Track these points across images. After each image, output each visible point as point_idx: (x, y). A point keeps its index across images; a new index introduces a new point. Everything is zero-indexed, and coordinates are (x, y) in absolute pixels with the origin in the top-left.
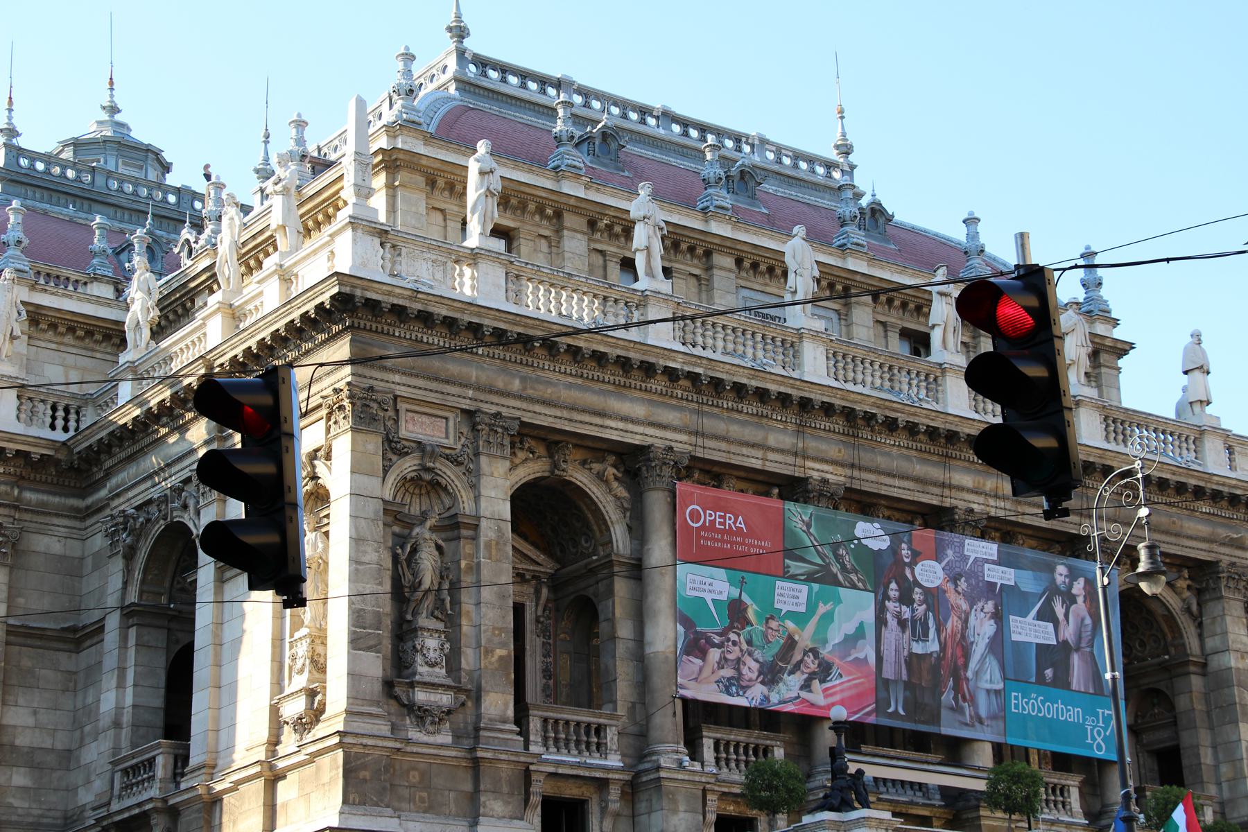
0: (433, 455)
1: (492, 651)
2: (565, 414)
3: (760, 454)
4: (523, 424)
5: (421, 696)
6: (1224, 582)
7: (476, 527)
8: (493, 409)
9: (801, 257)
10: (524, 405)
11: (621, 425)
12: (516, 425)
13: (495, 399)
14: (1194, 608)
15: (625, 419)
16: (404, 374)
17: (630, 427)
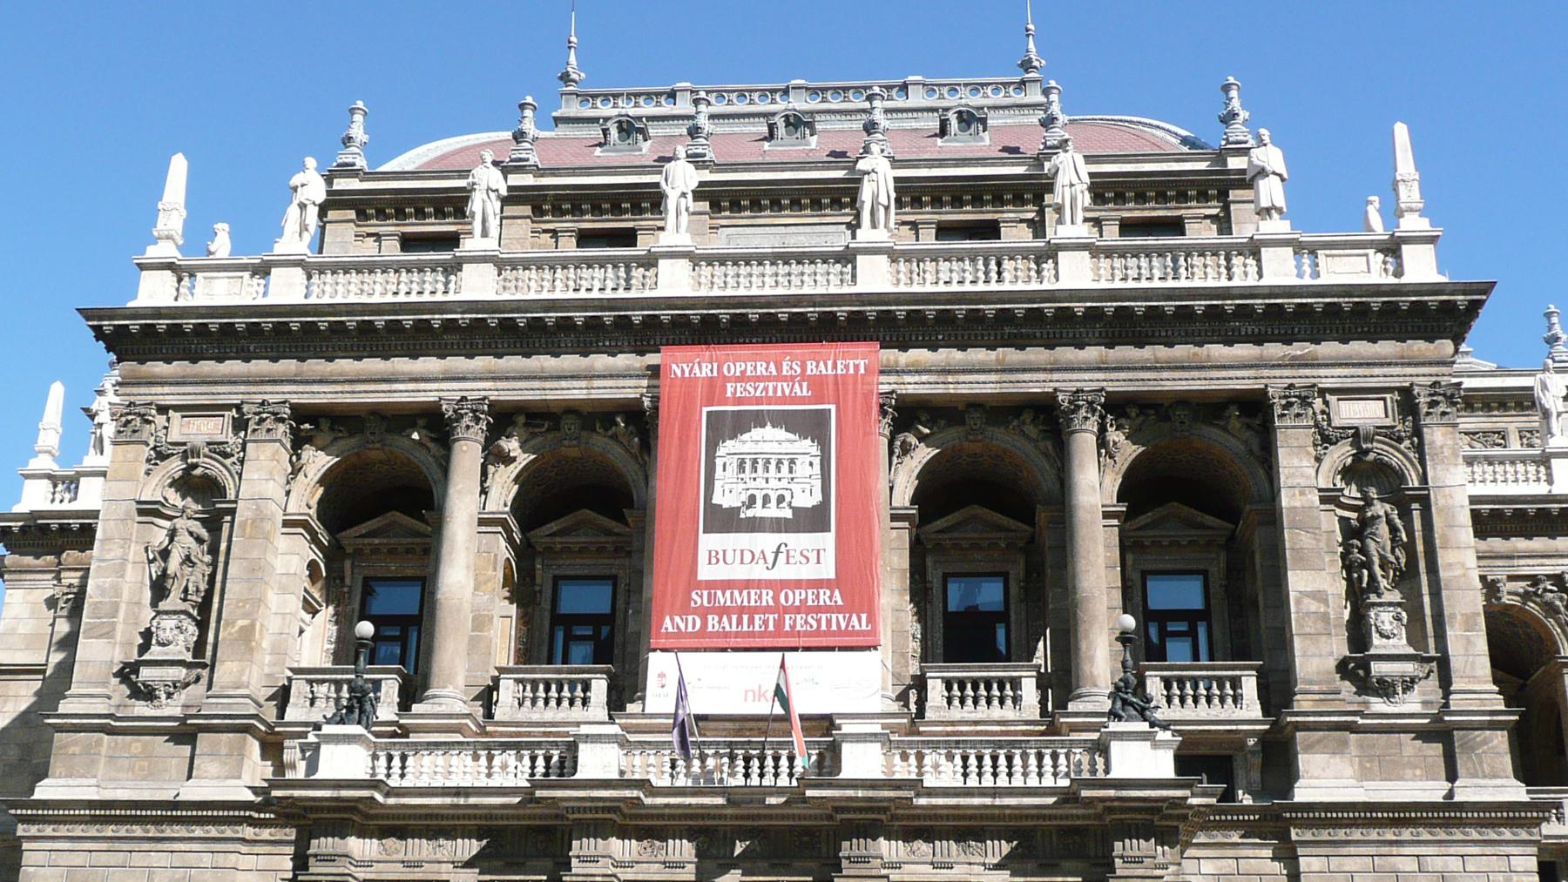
0: (195, 452)
1: (234, 622)
2: (347, 387)
3: (583, 384)
4: (295, 408)
5: (146, 673)
6: (1278, 411)
7: (232, 512)
8: (259, 398)
9: (681, 179)
10: (301, 388)
11: (411, 386)
12: (286, 411)
13: (269, 388)
14: (1256, 448)
15: (416, 380)
16: (171, 384)
17: (422, 386)
